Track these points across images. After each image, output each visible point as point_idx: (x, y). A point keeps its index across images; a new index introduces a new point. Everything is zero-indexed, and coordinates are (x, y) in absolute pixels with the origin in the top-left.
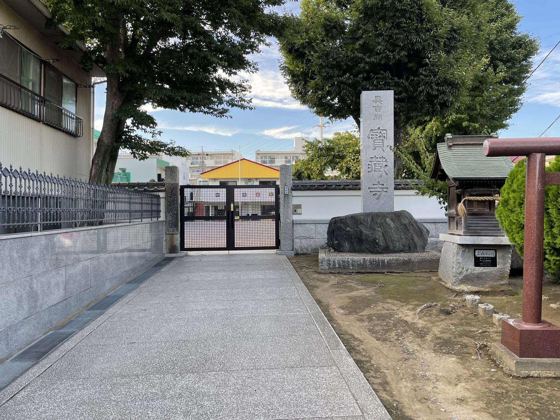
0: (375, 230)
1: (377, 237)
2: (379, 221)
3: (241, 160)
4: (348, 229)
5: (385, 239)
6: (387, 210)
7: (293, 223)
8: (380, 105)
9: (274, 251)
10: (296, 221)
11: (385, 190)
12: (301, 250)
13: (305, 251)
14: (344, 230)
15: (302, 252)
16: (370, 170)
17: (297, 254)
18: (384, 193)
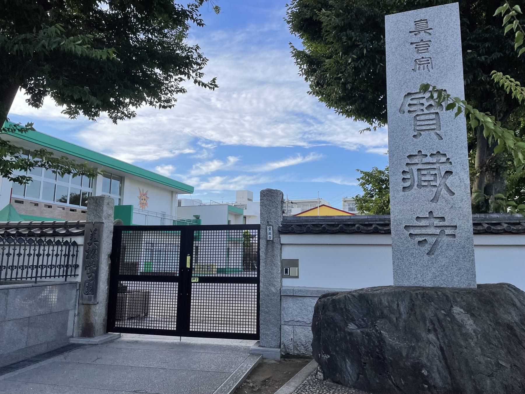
0: (418, 339)
1: (424, 360)
2: (429, 313)
3: (320, 206)
4: (352, 327)
5: (448, 367)
6: (458, 282)
7: (283, 295)
8: (426, 37)
9: (251, 344)
10: (285, 291)
11: (448, 231)
12: (295, 348)
13: (303, 351)
14: (340, 330)
15: (296, 352)
16: (407, 184)
17: (287, 356)
18: (445, 239)
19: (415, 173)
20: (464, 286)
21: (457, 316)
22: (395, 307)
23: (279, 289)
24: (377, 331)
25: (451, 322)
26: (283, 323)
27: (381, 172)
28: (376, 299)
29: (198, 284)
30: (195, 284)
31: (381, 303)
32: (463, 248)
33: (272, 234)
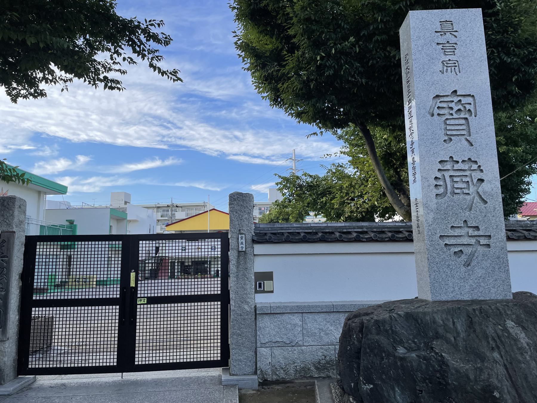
0: (483, 358)
1: (495, 382)
3: (210, 210)
4: (401, 350)
6: (494, 293)
7: (256, 313)
8: (453, 40)
9: (215, 372)
10: (262, 308)
11: (483, 241)
12: (274, 373)
13: (282, 375)
14: (389, 355)
15: (275, 377)
16: (441, 190)
17: (264, 383)
18: (481, 249)
19: (448, 180)
20: (500, 298)
21: (511, 331)
22: (451, 326)
23: (253, 307)
24: (437, 354)
25: (508, 337)
26: (259, 345)
27: (298, 178)
28: (428, 318)
29: (145, 306)
30: (142, 306)
31: (434, 322)
32: (498, 258)
33: (244, 243)
